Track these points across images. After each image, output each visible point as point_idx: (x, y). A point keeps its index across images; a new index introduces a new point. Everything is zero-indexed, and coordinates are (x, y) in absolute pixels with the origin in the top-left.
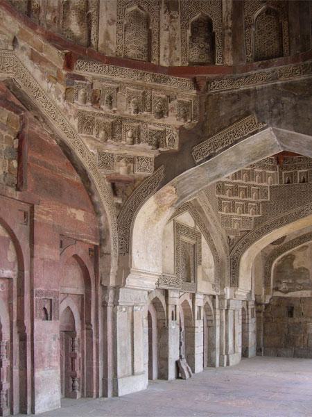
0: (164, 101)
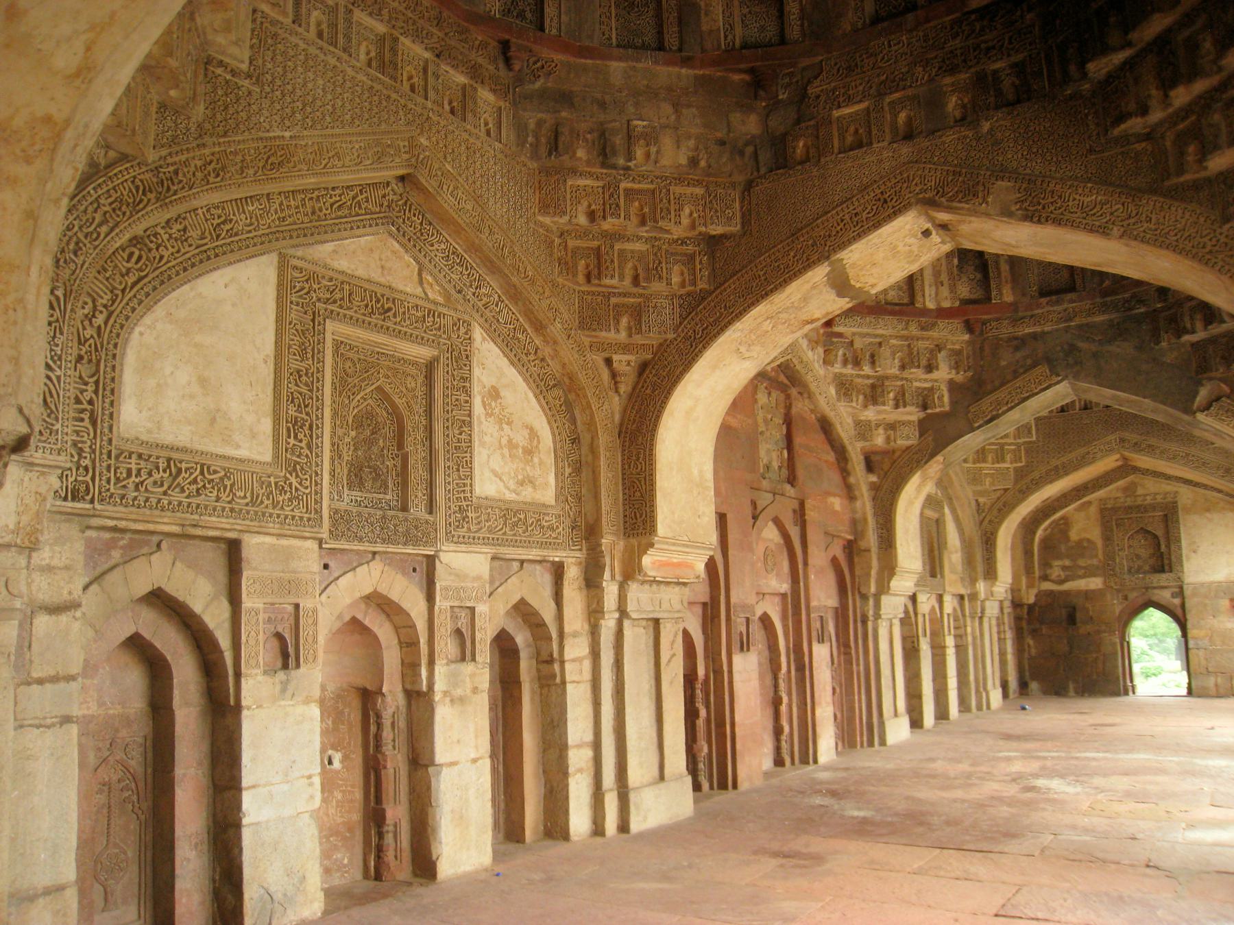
0: (932, 351)
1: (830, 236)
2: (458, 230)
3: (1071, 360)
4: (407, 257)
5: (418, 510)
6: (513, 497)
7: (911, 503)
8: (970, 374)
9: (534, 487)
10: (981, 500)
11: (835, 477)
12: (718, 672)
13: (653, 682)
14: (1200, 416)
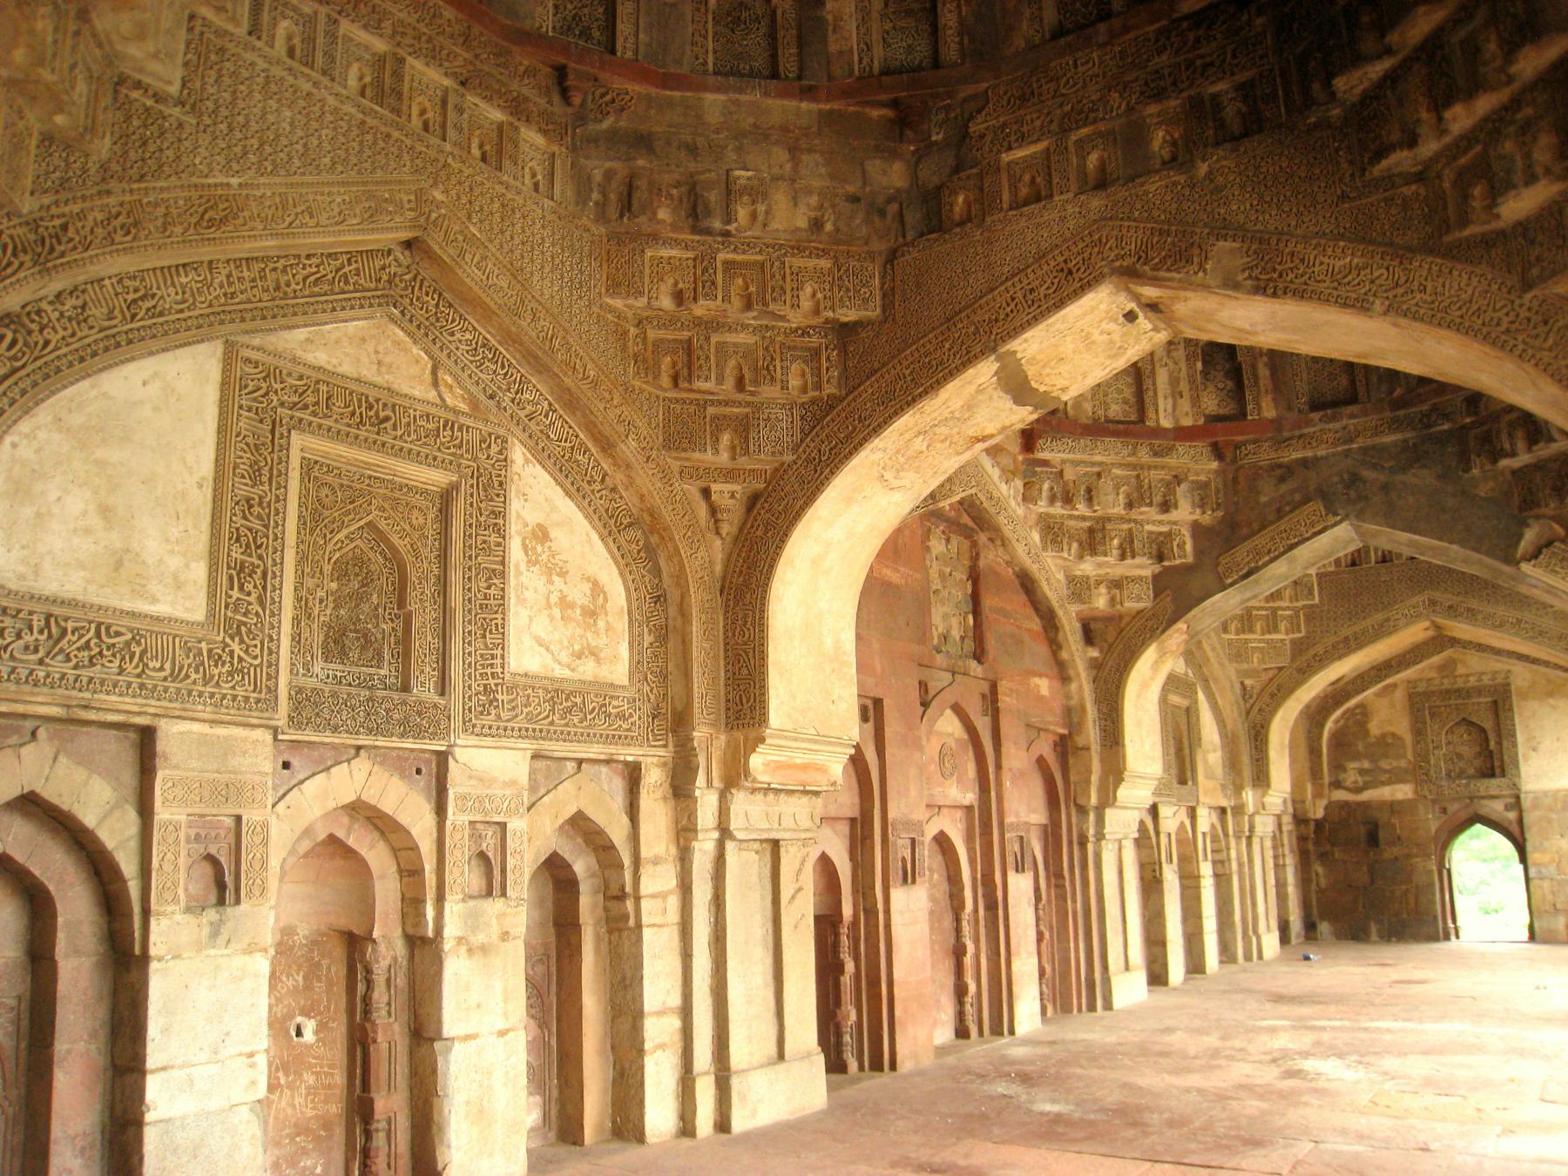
1: (997, 320)
2: (487, 314)
3: (1353, 494)
4: (415, 350)
5: (423, 690)
6: (566, 673)
7: (1145, 686)
8: (1220, 514)
9: (598, 661)
10: (1248, 682)
11: (1042, 650)
12: (871, 912)
13: (770, 926)
14: (1525, 567)
